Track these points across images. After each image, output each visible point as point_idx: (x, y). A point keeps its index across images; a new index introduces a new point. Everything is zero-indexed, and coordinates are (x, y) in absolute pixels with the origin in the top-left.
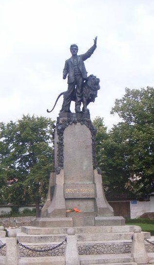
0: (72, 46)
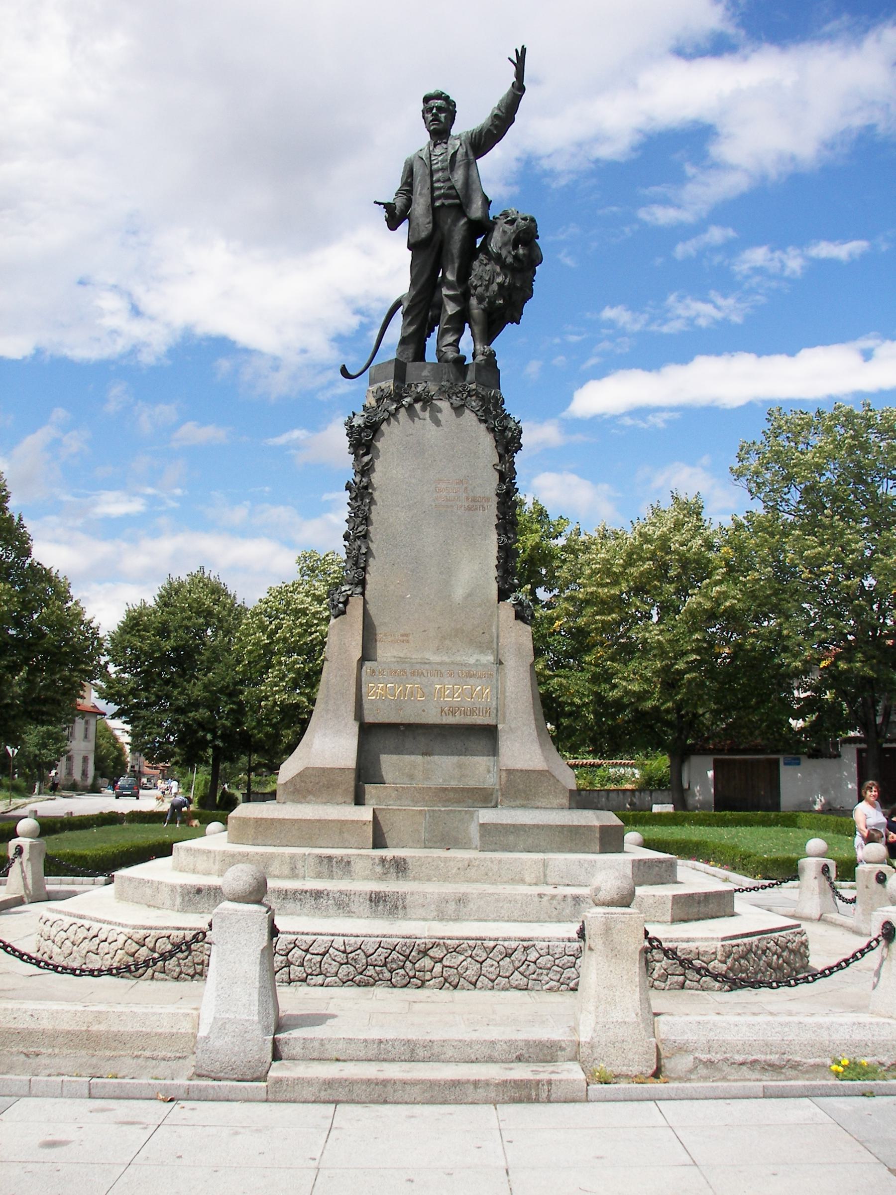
0: (427, 99)
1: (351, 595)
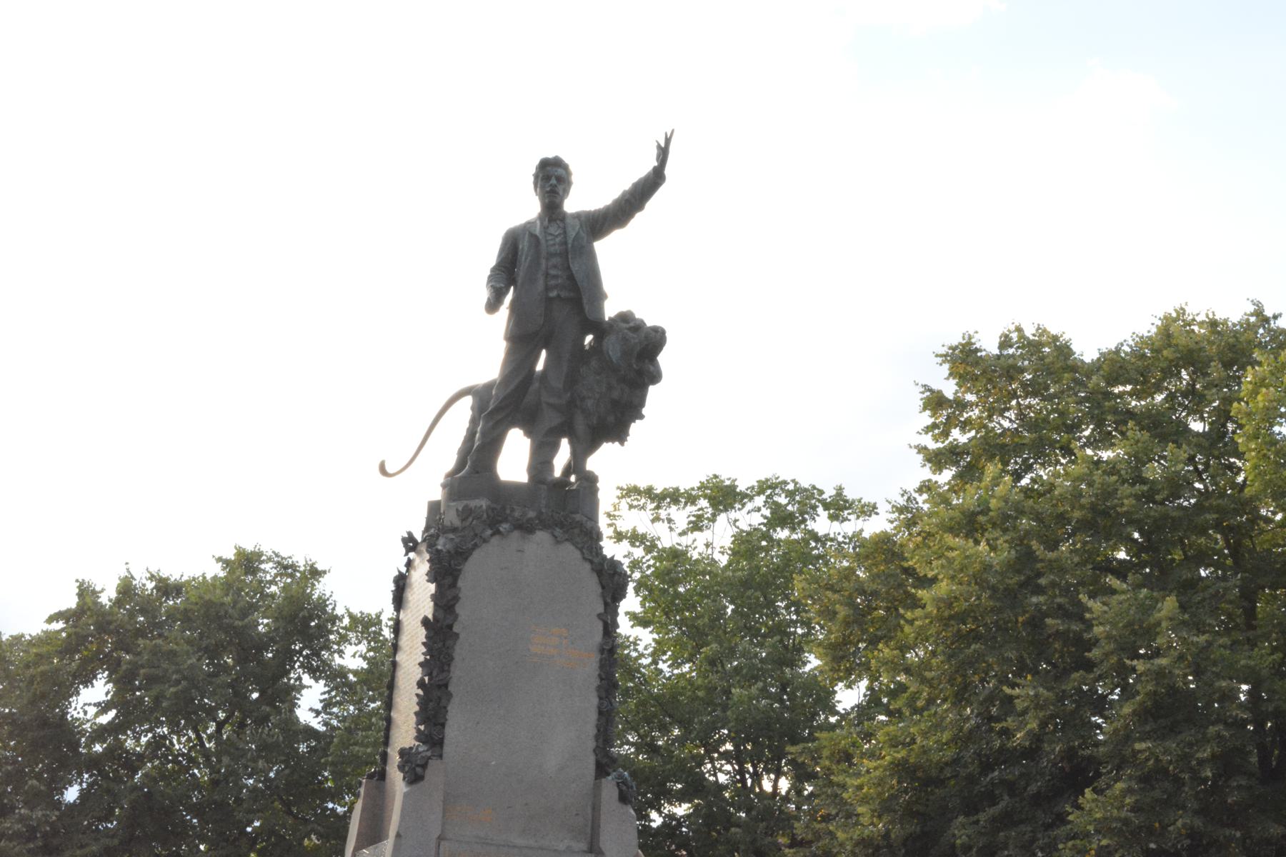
1: (429, 758)
